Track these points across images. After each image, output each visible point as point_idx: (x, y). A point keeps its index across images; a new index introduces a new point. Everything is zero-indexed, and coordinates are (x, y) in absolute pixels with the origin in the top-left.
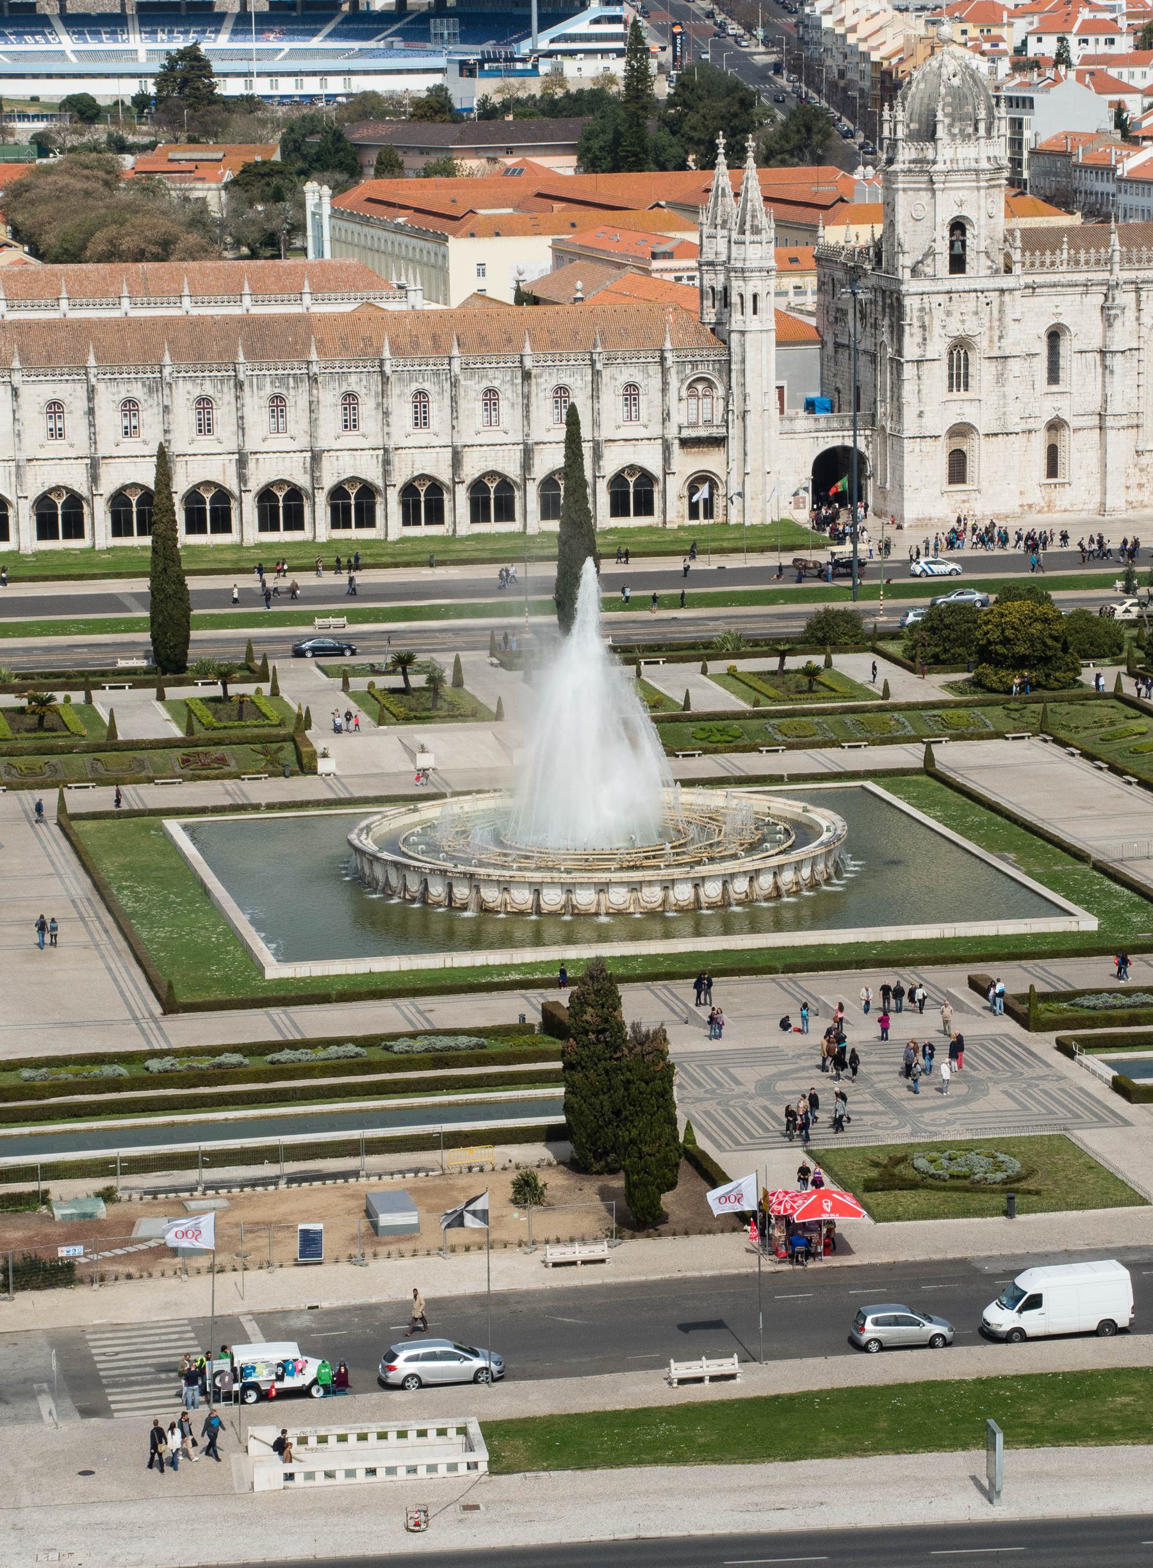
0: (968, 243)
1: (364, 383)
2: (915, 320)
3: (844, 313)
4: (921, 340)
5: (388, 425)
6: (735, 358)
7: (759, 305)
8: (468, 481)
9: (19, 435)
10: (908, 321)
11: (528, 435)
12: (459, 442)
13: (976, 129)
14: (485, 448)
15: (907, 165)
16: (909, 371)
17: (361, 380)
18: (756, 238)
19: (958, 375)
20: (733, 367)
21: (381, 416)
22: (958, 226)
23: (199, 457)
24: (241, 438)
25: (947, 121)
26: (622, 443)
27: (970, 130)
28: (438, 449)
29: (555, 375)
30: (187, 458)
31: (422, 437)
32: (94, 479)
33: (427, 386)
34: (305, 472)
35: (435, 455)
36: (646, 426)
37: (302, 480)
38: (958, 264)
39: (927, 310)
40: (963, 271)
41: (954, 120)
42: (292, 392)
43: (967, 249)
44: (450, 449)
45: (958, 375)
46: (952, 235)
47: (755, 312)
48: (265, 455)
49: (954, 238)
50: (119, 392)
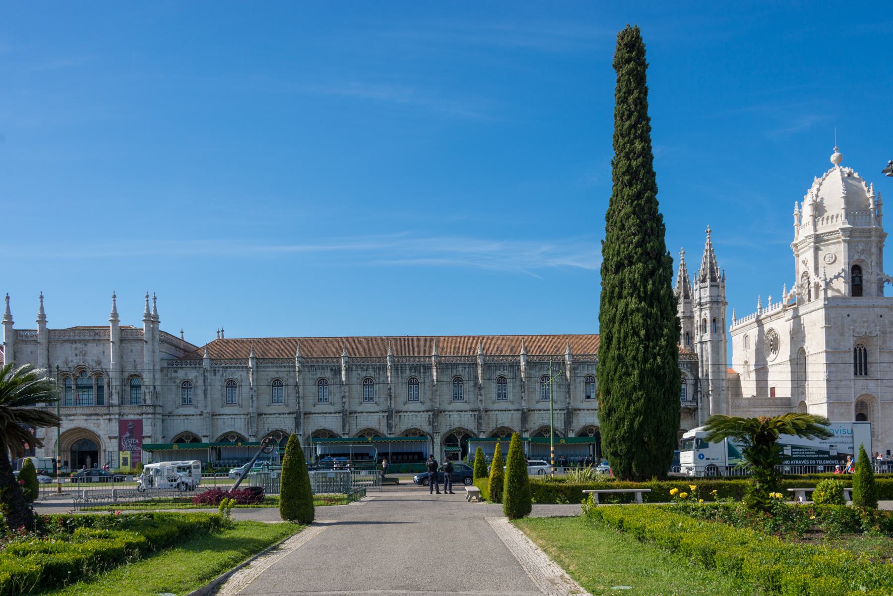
0: (864, 277)
1: (467, 370)
5: (481, 395)
8: (532, 431)
9: (252, 398)
11: (569, 403)
12: (524, 405)
14: (542, 412)
17: (465, 368)
21: (477, 390)
23: (365, 414)
24: (389, 402)
28: (512, 412)
29: (586, 369)
30: (357, 414)
31: (502, 405)
32: (297, 425)
33: (506, 372)
34: (430, 424)
35: (510, 415)
37: (426, 428)
42: (422, 374)
43: (864, 282)
44: (520, 412)
46: (853, 273)
48: (405, 414)
49: (854, 275)
50: (317, 374)
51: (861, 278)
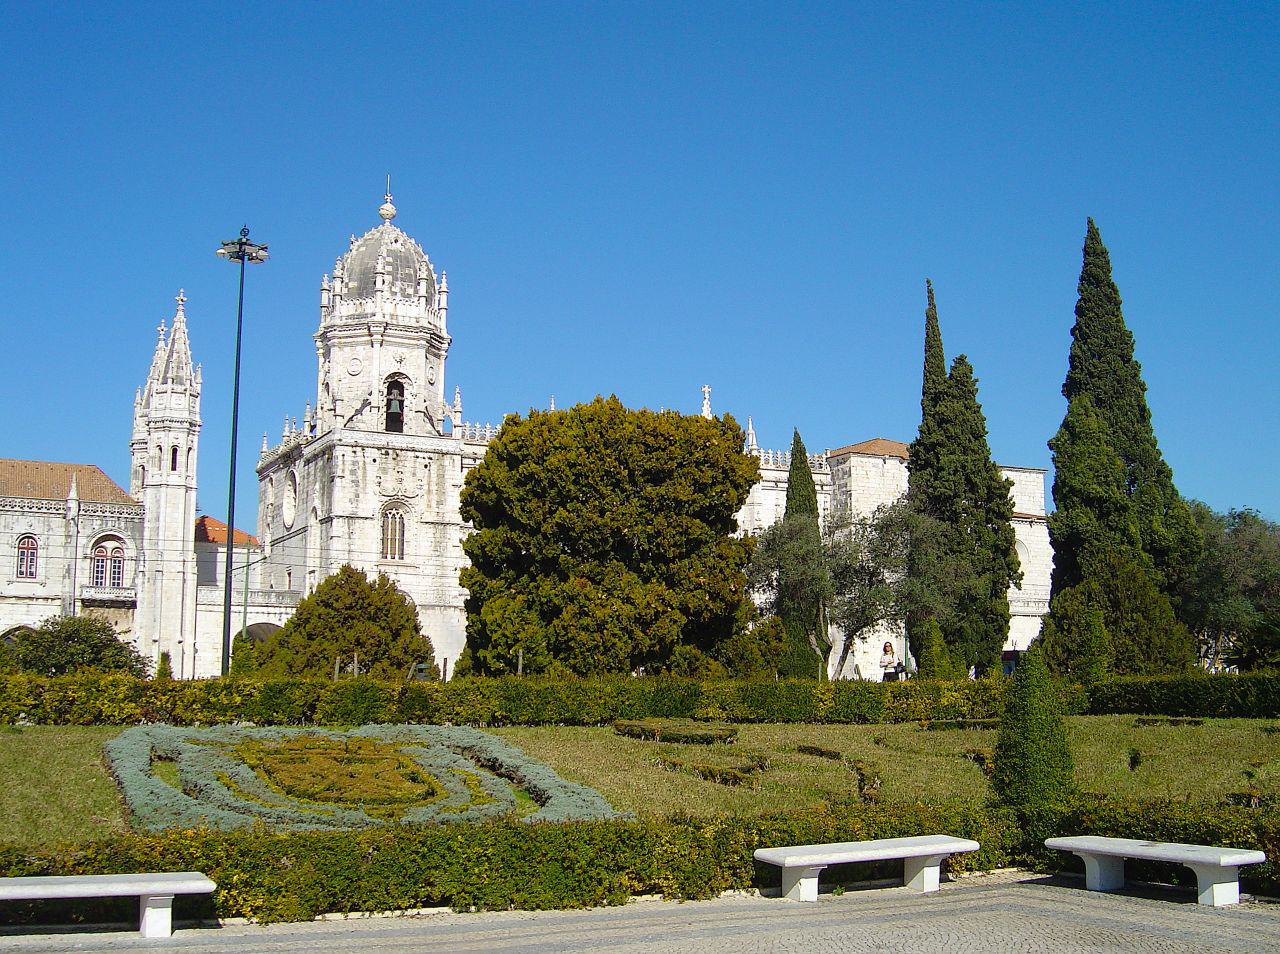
2: (347, 473)
3: (280, 507)
4: (352, 496)
6: (147, 517)
7: (181, 458)
10: (339, 473)
13: (416, 292)
15: (344, 321)
16: (338, 527)
18: (180, 388)
19: (393, 540)
20: (146, 524)
22: (395, 384)
25: (388, 278)
26: (13, 600)
27: (410, 291)
36: (43, 584)
38: (394, 422)
39: (361, 464)
40: (400, 430)
41: (395, 279)
45: (393, 540)
46: (389, 393)
47: (174, 468)
49: (391, 397)
51: (401, 403)
